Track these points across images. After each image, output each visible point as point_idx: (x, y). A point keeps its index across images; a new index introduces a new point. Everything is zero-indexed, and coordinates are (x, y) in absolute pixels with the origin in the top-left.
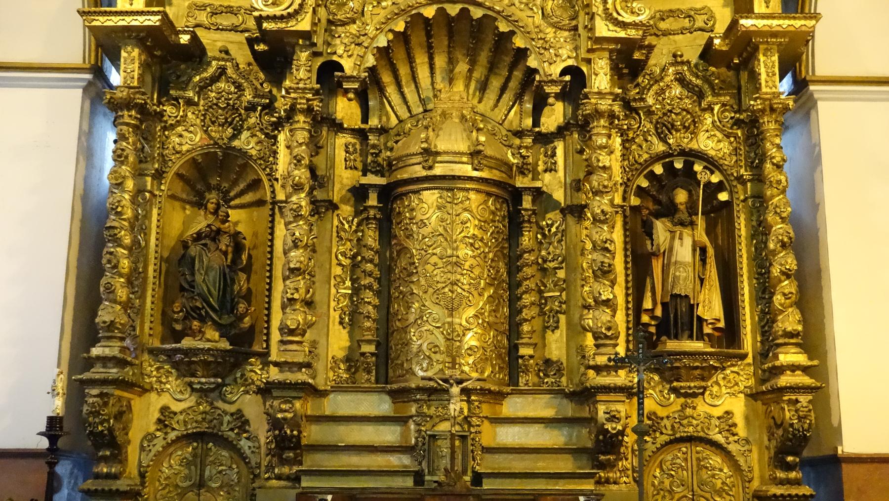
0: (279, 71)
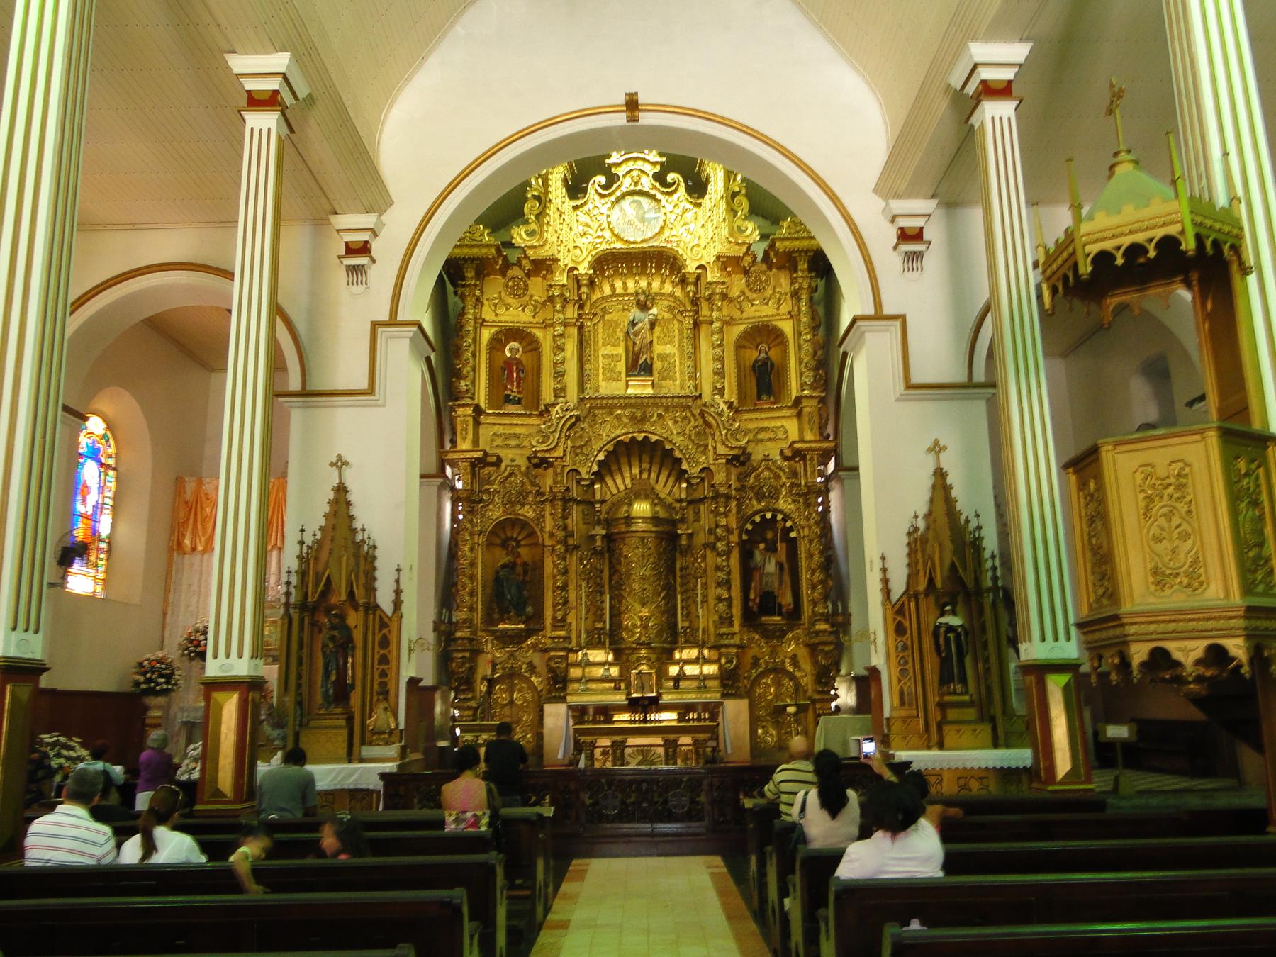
0: (548, 480)
